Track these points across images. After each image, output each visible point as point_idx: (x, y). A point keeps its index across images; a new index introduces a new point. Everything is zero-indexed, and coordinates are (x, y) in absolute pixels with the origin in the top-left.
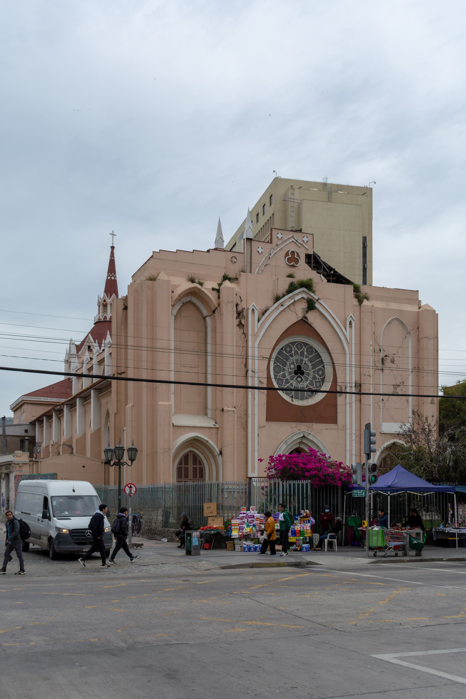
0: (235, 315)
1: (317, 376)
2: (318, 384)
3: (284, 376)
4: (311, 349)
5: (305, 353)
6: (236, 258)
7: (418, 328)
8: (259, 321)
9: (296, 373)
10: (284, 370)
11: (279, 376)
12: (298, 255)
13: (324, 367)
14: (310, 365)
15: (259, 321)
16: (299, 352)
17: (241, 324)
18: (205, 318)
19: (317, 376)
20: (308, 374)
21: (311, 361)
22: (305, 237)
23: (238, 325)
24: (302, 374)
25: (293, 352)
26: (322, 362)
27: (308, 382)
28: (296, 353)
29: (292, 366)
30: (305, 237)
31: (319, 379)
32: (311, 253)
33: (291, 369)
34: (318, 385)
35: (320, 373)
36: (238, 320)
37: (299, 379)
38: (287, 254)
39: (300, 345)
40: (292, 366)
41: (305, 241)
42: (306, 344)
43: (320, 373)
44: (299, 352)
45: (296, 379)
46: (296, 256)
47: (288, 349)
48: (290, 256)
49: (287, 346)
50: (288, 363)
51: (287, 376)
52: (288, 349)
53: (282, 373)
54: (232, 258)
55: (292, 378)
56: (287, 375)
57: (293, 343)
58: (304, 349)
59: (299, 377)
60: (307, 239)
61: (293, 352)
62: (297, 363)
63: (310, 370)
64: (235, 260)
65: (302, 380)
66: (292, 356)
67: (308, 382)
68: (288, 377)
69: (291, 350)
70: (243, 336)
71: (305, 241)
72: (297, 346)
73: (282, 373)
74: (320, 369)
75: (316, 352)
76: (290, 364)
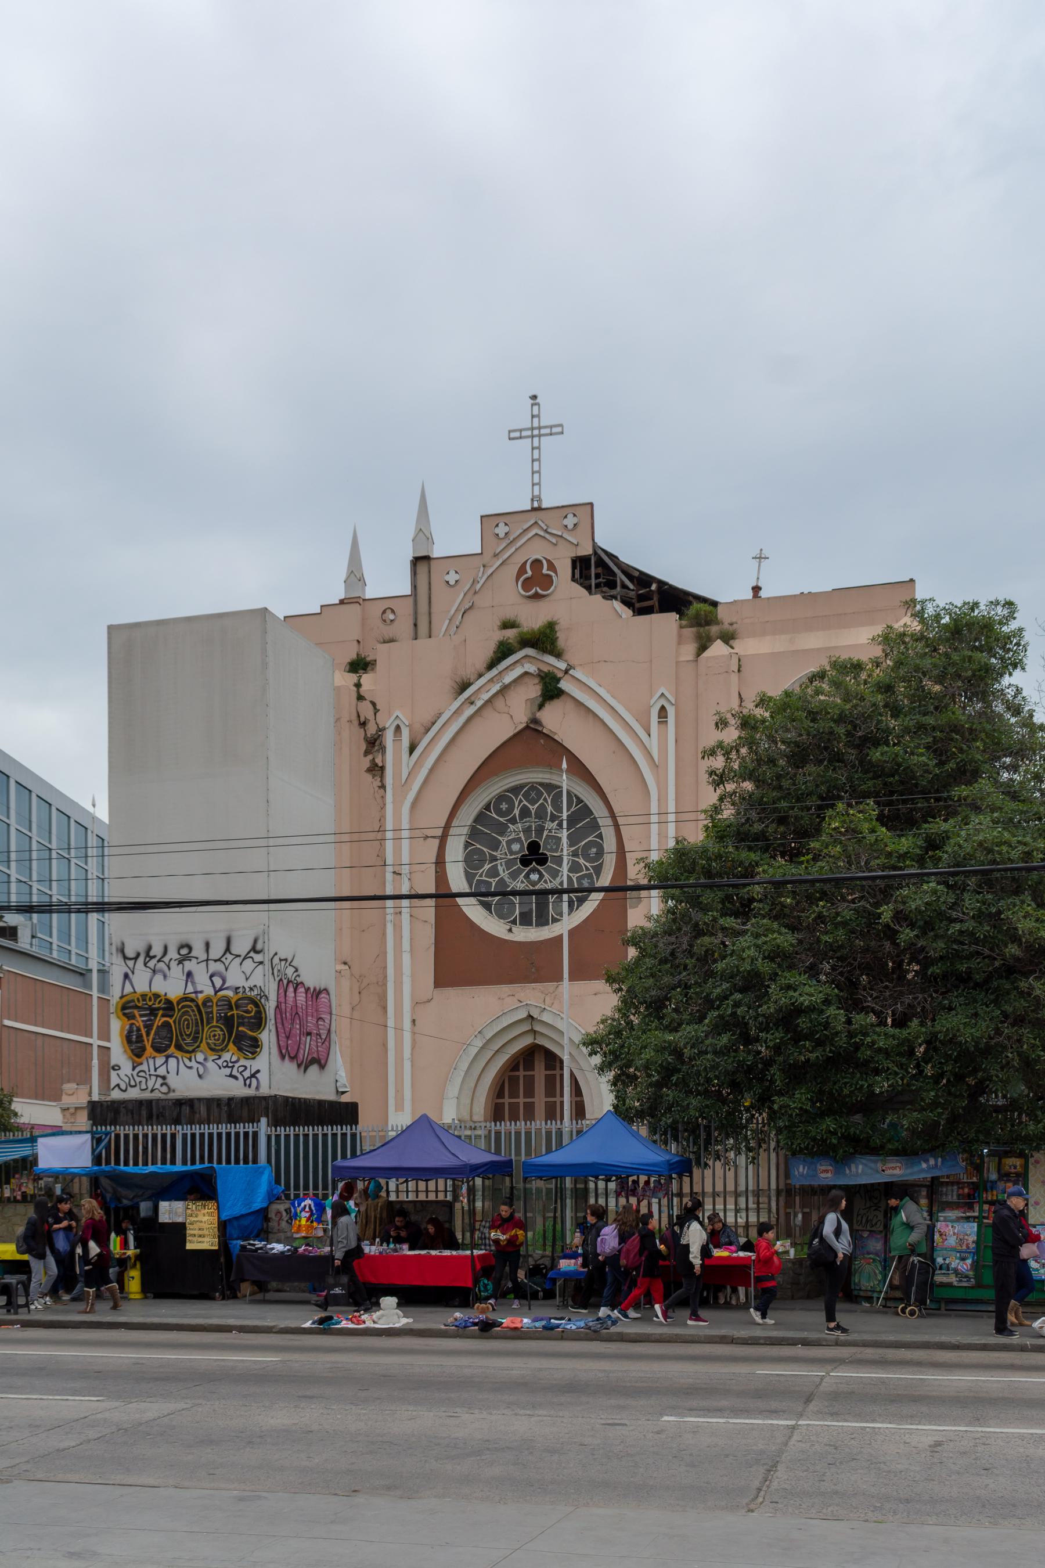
9: (525, 862)
16: (533, 808)
25: (517, 812)
28: (525, 813)
39: (532, 791)
40: (516, 847)
44: (533, 808)
47: (504, 806)
49: (501, 798)
50: (504, 840)
52: (504, 806)
57: (516, 790)
58: (545, 800)
66: (513, 821)
72: (526, 796)
76: (509, 843)
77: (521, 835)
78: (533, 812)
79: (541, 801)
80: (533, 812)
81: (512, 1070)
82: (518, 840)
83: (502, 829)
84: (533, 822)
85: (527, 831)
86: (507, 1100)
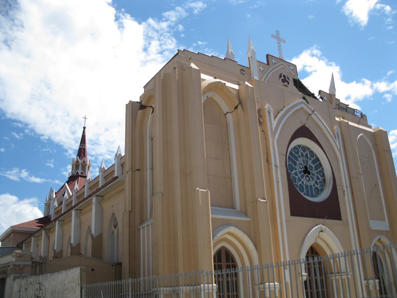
1: (319, 176)
5: (309, 155)
10: (296, 169)
12: (288, 79)
13: (323, 169)
14: (313, 166)
16: (304, 154)
18: (226, 114)
19: (319, 176)
20: (313, 174)
24: (309, 173)
25: (300, 153)
26: (320, 165)
28: (302, 155)
29: (301, 166)
31: (321, 180)
33: (301, 168)
34: (321, 185)
35: (321, 175)
38: (280, 76)
40: (301, 166)
44: (304, 154)
45: (306, 178)
47: (296, 151)
48: (283, 78)
50: (298, 163)
51: (298, 174)
52: (296, 151)
53: (294, 171)
55: (302, 176)
56: (298, 173)
59: (307, 176)
61: (300, 153)
62: (304, 164)
65: (309, 179)
69: (298, 153)
70: (262, 132)
72: (302, 148)
73: (294, 171)
74: (320, 171)
75: (316, 156)
77: (302, 162)
78: (304, 155)
79: (306, 152)
80: (304, 155)
82: (301, 164)
83: (297, 159)
85: (304, 161)
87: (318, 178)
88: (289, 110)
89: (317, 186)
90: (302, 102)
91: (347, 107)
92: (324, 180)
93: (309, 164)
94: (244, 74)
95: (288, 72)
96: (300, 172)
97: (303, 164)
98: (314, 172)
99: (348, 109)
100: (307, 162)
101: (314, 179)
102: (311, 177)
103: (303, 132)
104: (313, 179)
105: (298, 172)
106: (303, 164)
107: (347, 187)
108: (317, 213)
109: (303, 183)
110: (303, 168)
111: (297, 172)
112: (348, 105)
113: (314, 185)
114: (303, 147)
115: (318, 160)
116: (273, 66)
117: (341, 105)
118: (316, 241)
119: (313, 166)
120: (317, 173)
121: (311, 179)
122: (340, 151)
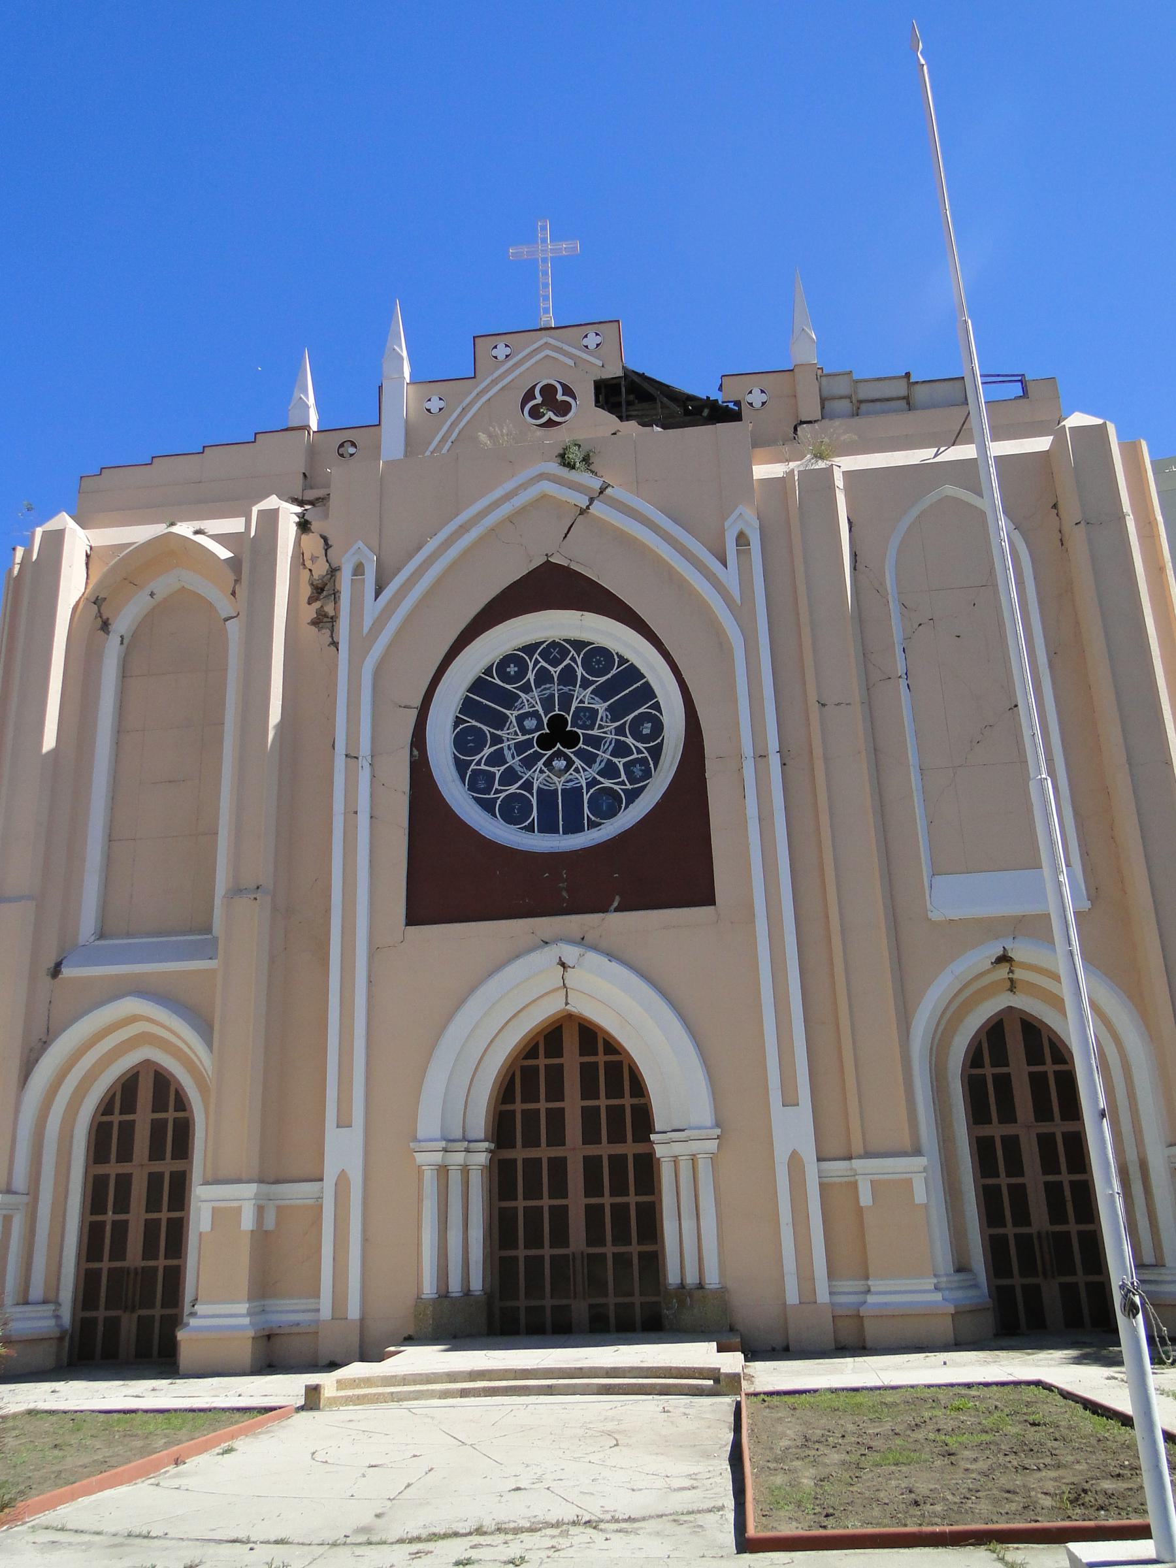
0: (306, 591)
1: (630, 740)
2: (637, 770)
3: (497, 758)
4: (598, 658)
5: (580, 671)
6: (354, 445)
7: (1055, 506)
8: (378, 594)
10: (497, 740)
11: (478, 763)
12: (568, 391)
15: (378, 594)
16: (555, 671)
17: (326, 616)
21: (602, 693)
22: (592, 335)
23: (315, 623)
24: (571, 740)
25: (531, 676)
27: (597, 767)
28: (543, 677)
29: (530, 723)
30: (592, 335)
32: (614, 371)
36: (317, 605)
37: (560, 764)
39: (554, 651)
41: (592, 346)
42: (579, 645)
43: (646, 731)
44: (555, 671)
46: (560, 397)
47: (512, 669)
50: (512, 715)
52: (512, 669)
53: (487, 751)
54: (342, 445)
55: (529, 763)
56: (508, 754)
57: (530, 649)
58: (573, 659)
59: (559, 755)
60: (599, 339)
61: (531, 676)
63: (600, 727)
64: (352, 450)
65: (570, 763)
66: (526, 689)
67: (597, 767)
68: (513, 761)
70: (333, 648)
71: (592, 346)
72: (545, 655)
73: (487, 751)
75: (623, 660)
76: (520, 719)
77: (539, 708)
81: (526, 1057)
82: (535, 714)
83: (510, 700)
84: (555, 689)
85: (547, 702)
86: (519, 1106)
87: (621, 750)
88: (464, 529)
89: (607, 783)
90: (542, 476)
91: (911, 385)
92: (656, 752)
93: (574, 705)
94: (351, 455)
95: (571, 363)
96: (521, 747)
97: (541, 712)
98: (606, 730)
99: (920, 393)
100: (566, 700)
101: (598, 760)
102: (581, 754)
103: (552, 586)
104: (589, 759)
105: (509, 749)
106: (541, 712)
107: (761, 757)
108: (564, 894)
109: (528, 786)
110: (540, 726)
111: (506, 751)
112: (908, 375)
113: (592, 783)
114: (554, 644)
115: (633, 674)
116: (497, 368)
117: (864, 392)
118: (567, 1004)
119: (601, 707)
120: (620, 731)
121: (578, 763)
122: (742, 612)
